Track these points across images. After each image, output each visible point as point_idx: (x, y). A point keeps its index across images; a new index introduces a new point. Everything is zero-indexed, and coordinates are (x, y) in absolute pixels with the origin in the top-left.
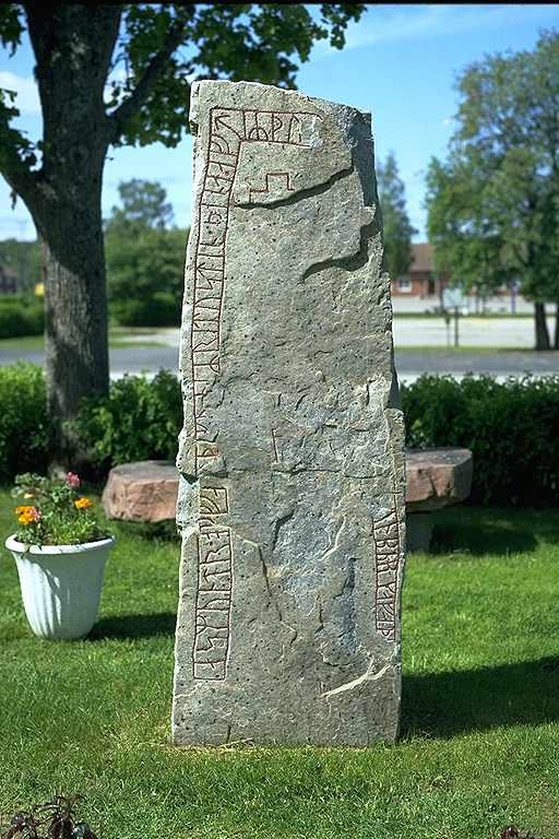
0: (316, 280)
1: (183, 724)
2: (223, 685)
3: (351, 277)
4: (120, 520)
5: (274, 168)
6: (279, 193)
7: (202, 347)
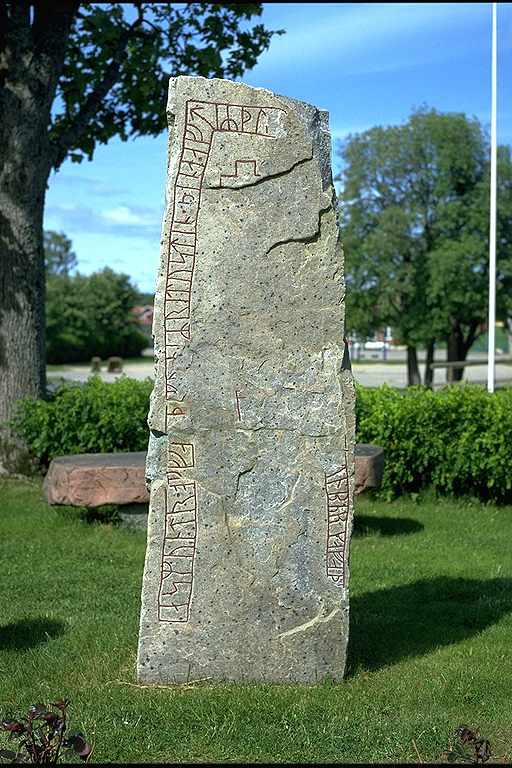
0: (281, 256)
1: (148, 664)
2: (185, 627)
3: (309, 253)
4: (61, 505)
5: (243, 155)
6: (247, 178)
7: (174, 315)
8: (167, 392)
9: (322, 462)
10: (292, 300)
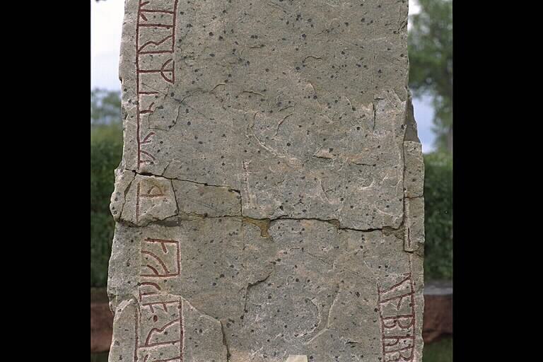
8: (140, 162)
9: (375, 269)
10: (328, 24)
